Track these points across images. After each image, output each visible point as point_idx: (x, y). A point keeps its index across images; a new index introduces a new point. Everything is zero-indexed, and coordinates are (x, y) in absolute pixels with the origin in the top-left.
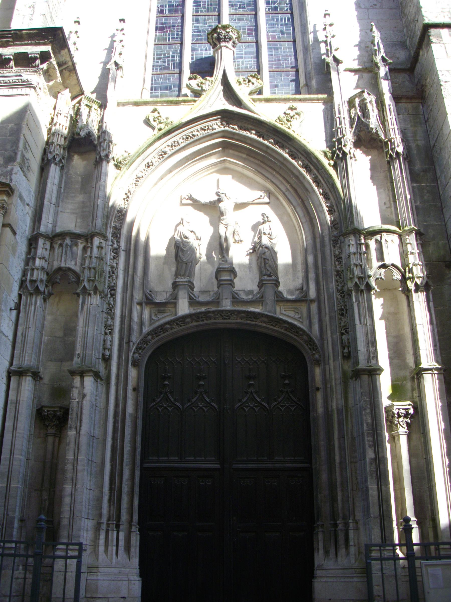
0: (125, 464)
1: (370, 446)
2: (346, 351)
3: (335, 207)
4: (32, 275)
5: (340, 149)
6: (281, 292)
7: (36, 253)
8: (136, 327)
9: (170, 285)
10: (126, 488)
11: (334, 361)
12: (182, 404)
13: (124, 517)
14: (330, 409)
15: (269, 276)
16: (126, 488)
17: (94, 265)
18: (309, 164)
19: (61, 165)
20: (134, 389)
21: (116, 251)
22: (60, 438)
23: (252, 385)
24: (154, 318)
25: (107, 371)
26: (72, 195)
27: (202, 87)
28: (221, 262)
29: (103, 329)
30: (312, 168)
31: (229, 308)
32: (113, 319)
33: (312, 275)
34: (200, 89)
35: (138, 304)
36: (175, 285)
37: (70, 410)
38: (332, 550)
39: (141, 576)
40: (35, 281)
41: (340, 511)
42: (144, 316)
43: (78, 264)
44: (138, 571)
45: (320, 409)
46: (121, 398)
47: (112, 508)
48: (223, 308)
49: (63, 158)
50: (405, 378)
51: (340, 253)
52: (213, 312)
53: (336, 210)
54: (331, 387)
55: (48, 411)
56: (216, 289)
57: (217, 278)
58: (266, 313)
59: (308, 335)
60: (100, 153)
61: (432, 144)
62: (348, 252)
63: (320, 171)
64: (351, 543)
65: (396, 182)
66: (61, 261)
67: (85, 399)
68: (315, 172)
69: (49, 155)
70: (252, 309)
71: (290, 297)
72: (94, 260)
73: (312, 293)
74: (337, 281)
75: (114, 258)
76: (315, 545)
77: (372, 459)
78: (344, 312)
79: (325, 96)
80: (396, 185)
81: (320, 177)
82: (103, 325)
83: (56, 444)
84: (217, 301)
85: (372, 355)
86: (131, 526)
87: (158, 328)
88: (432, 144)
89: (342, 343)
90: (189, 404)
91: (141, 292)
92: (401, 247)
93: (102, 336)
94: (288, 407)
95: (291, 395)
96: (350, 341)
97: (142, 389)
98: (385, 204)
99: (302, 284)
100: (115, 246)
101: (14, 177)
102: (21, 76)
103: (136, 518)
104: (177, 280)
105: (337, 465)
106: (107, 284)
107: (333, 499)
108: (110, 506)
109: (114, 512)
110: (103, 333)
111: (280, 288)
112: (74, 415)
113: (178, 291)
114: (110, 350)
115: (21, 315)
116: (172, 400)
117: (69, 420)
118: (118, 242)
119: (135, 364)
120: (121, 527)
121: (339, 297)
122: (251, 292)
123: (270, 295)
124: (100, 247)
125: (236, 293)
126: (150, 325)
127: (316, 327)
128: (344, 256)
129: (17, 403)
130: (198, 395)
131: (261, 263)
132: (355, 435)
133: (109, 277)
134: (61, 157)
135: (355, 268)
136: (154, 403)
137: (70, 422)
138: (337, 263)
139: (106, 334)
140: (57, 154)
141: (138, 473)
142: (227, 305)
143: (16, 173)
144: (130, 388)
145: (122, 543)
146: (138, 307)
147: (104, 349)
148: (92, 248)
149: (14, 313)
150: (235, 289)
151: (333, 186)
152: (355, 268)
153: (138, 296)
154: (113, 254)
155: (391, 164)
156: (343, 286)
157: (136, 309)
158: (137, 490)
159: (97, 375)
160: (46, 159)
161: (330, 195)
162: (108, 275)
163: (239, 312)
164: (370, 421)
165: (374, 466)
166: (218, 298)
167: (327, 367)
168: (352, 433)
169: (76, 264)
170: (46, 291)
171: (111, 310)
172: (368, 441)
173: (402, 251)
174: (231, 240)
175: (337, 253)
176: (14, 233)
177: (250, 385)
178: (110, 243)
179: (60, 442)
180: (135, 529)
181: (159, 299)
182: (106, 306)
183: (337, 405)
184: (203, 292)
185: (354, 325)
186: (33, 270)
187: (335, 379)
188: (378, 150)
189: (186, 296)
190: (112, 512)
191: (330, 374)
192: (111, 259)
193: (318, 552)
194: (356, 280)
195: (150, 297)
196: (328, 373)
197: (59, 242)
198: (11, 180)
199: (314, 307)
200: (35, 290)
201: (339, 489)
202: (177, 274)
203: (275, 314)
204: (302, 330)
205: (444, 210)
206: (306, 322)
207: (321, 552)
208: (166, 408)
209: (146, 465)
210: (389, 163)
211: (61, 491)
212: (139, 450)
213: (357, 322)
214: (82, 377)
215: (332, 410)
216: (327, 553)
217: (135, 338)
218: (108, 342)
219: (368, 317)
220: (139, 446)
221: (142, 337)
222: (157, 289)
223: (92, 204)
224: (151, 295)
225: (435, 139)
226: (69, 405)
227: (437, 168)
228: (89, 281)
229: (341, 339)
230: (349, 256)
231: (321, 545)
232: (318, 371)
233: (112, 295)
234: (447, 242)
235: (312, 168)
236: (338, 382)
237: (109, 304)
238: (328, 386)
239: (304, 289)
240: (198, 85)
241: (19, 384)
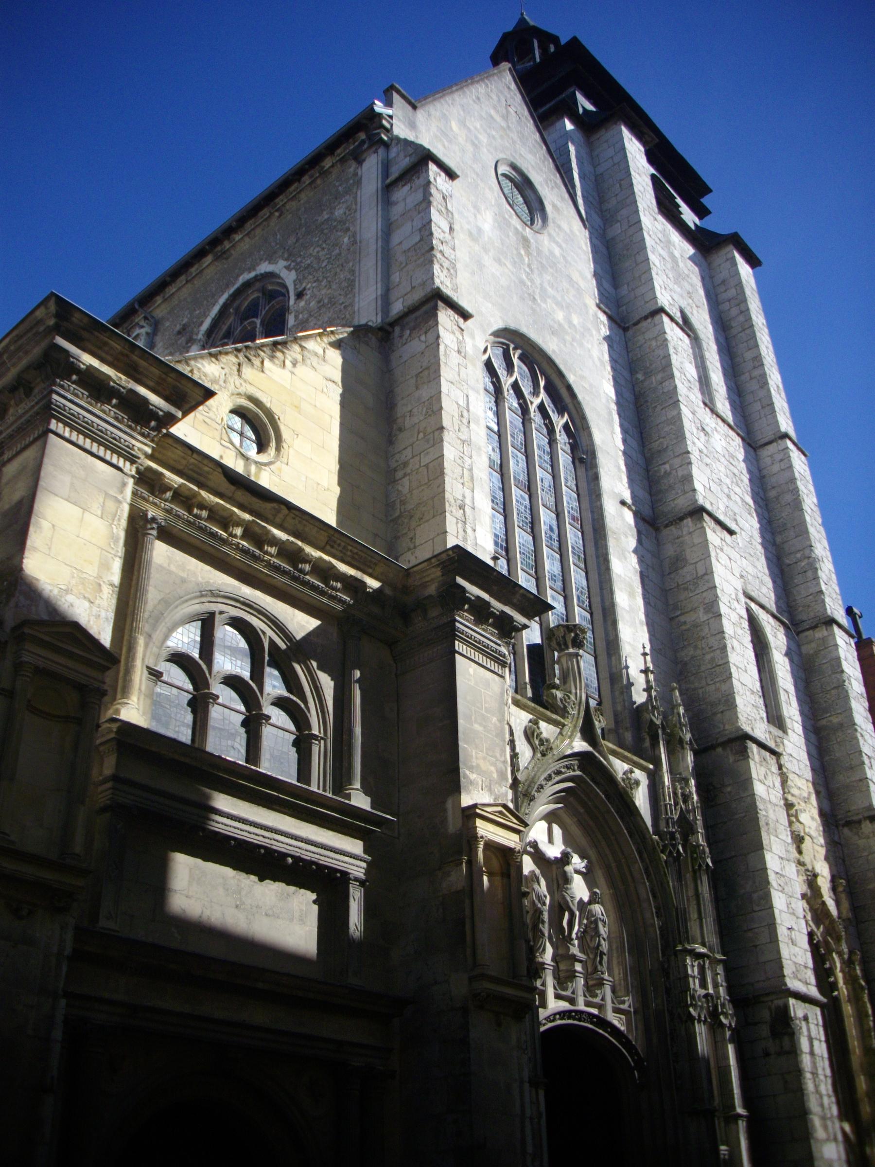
3: (662, 911)
5: (675, 846)
18: (644, 850)
27: (565, 707)
34: (562, 706)
65: (703, 897)
68: (647, 860)
79: (651, 767)
80: (703, 900)
81: (650, 869)
102: (499, 645)
151: (664, 886)
155: (698, 874)
210: (694, 871)
235: (645, 855)
240: (561, 700)
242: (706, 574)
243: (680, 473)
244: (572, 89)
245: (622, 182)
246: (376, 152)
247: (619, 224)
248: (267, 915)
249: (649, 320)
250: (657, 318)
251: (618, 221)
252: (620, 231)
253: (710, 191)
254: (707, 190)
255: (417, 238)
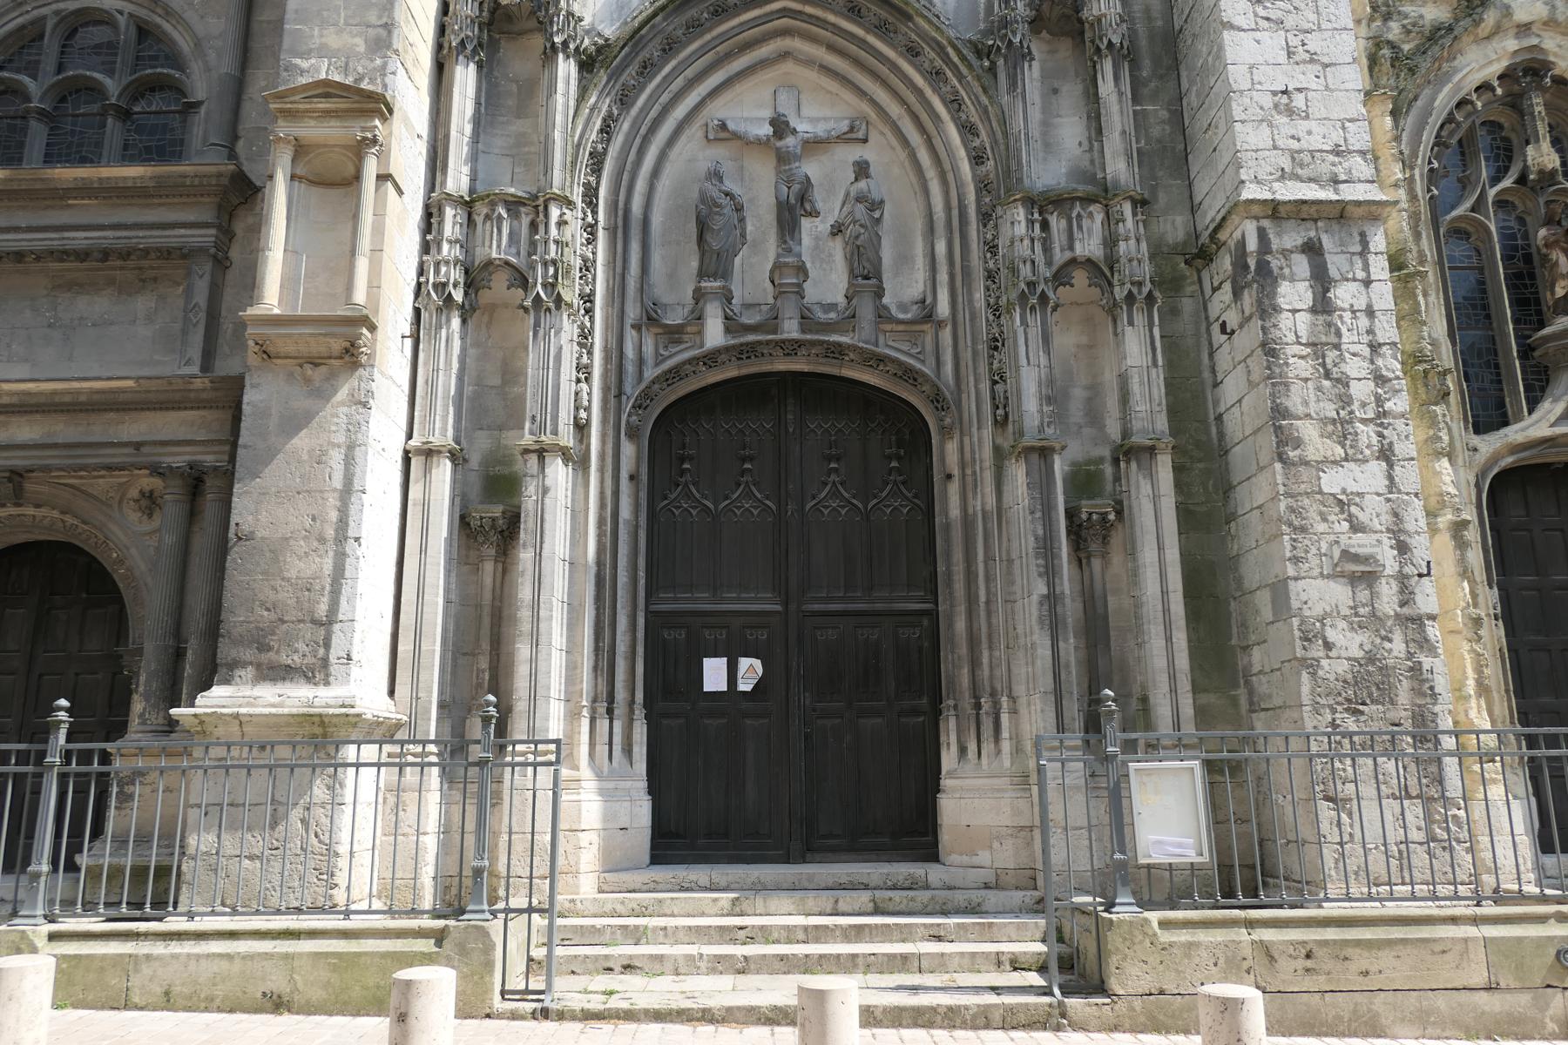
0: (619, 606)
1: (1040, 575)
2: (1000, 412)
4: (437, 272)
6: (886, 308)
7: (440, 232)
8: (630, 368)
9: (690, 293)
10: (622, 647)
11: (979, 428)
12: (716, 504)
13: (621, 694)
14: (970, 511)
15: (866, 278)
16: (622, 647)
17: (553, 254)
18: (944, 66)
19: (477, 58)
20: (632, 478)
21: (591, 229)
22: (504, 563)
23: (836, 470)
24: (662, 352)
25: (584, 447)
26: (501, 119)
28: (780, 250)
29: (574, 373)
30: (949, 74)
31: (795, 335)
32: (590, 353)
33: (943, 277)
35: (633, 326)
36: (699, 295)
37: (523, 515)
38: (972, 747)
39: (649, 793)
40: (444, 285)
41: (986, 682)
42: (644, 348)
43: (523, 253)
44: (643, 784)
45: (955, 512)
46: (609, 493)
47: (600, 680)
48: (785, 336)
49: (480, 45)
50: (1101, 460)
51: (995, 237)
52: (768, 342)
53: (990, 156)
54: (974, 473)
55: (481, 518)
56: (771, 301)
57: (773, 282)
58: (861, 345)
59: (935, 385)
60: (552, 36)
61: (1177, 27)
62: (1009, 234)
63: (964, 82)
64: (1005, 734)
66: (491, 247)
67: (549, 495)
69: (452, 37)
70: (835, 338)
71: (901, 316)
72: (553, 247)
73: (943, 308)
74: (987, 289)
75: (589, 242)
76: (943, 738)
77: (1043, 596)
78: (999, 344)
81: (963, 93)
82: (574, 365)
83: (499, 575)
84: (772, 323)
85: (1046, 420)
86: (632, 711)
87: (670, 371)
88: (1177, 27)
89: (994, 398)
90: (727, 502)
91: (639, 305)
92: (1106, 227)
93: (574, 384)
94: (895, 508)
95: (902, 487)
96: (1009, 395)
97: (644, 477)
98: (1080, 144)
99: (924, 292)
100: (590, 219)
101: (389, 79)
103: (639, 696)
104: (703, 284)
105: (982, 606)
106: (577, 292)
107: (975, 664)
108: (596, 678)
109: (603, 688)
110: (574, 379)
111: (885, 300)
112: (531, 524)
113: (705, 303)
114: (588, 409)
115: (421, 346)
116: (697, 495)
117: (522, 532)
118: (595, 213)
119: (633, 434)
120: (616, 712)
121: (991, 318)
122: (832, 307)
123: (866, 311)
124: (562, 223)
125: (808, 310)
126: (657, 365)
127: (948, 368)
128: (1002, 243)
129: (425, 506)
130: (742, 487)
131: (852, 254)
132: (1014, 555)
133: (581, 278)
134: (475, 42)
135: (1021, 266)
136: (666, 502)
137: (522, 535)
138: (989, 255)
139: (578, 381)
140: (467, 37)
141: (641, 621)
142: (791, 329)
143: (394, 73)
144: (624, 475)
145: (617, 739)
146: (634, 333)
147: (577, 409)
148: (547, 225)
149: (409, 343)
150: (805, 300)
152: (1021, 266)
153: (633, 312)
154: (585, 234)
156: (998, 297)
157: (630, 336)
158: (640, 650)
159: (565, 454)
160: (446, 45)
161: (980, 126)
162: (578, 275)
163: (813, 343)
164: (1040, 532)
165: (1046, 607)
166: (776, 318)
167: (967, 440)
168: (1008, 552)
169: (518, 253)
170: (466, 303)
171: (586, 338)
172: (1037, 565)
173: (1107, 233)
174: (799, 211)
175: (989, 236)
176: (400, 192)
177: (831, 471)
178: (580, 215)
179: (505, 571)
180: (639, 713)
181: (673, 319)
182: (577, 331)
183: (983, 504)
184: (747, 306)
185: (1018, 368)
186: (437, 265)
187: (981, 461)
188: (1073, 38)
189: (720, 313)
190: (600, 687)
191: (973, 452)
192: (582, 245)
193: (949, 748)
194: (1023, 286)
195: (655, 315)
196: (967, 449)
197: (485, 211)
198: (385, 86)
199: (946, 335)
200: (444, 301)
201: (985, 645)
202: (702, 274)
203: (877, 346)
204: (924, 375)
205: (1190, 157)
206: (931, 361)
207: (954, 748)
208: (686, 509)
209: (653, 608)
211: (511, 655)
212: (642, 582)
213: (1023, 361)
214: (541, 459)
215: (975, 514)
216: (963, 750)
217: (632, 390)
218: (585, 396)
219: (1041, 353)
220: (642, 574)
221: (643, 386)
222: (666, 299)
223: (542, 139)
224: (656, 312)
225: (1184, 17)
226: (520, 507)
227: (1184, 74)
228: (544, 285)
229: (993, 391)
230: (1012, 243)
231: (953, 738)
232: (952, 447)
233: (587, 311)
234: (1191, 217)
235: (949, 74)
236: (987, 464)
237: (582, 327)
238: (969, 471)
239: (928, 302)
241: (427, 471)
248: (93, 325)
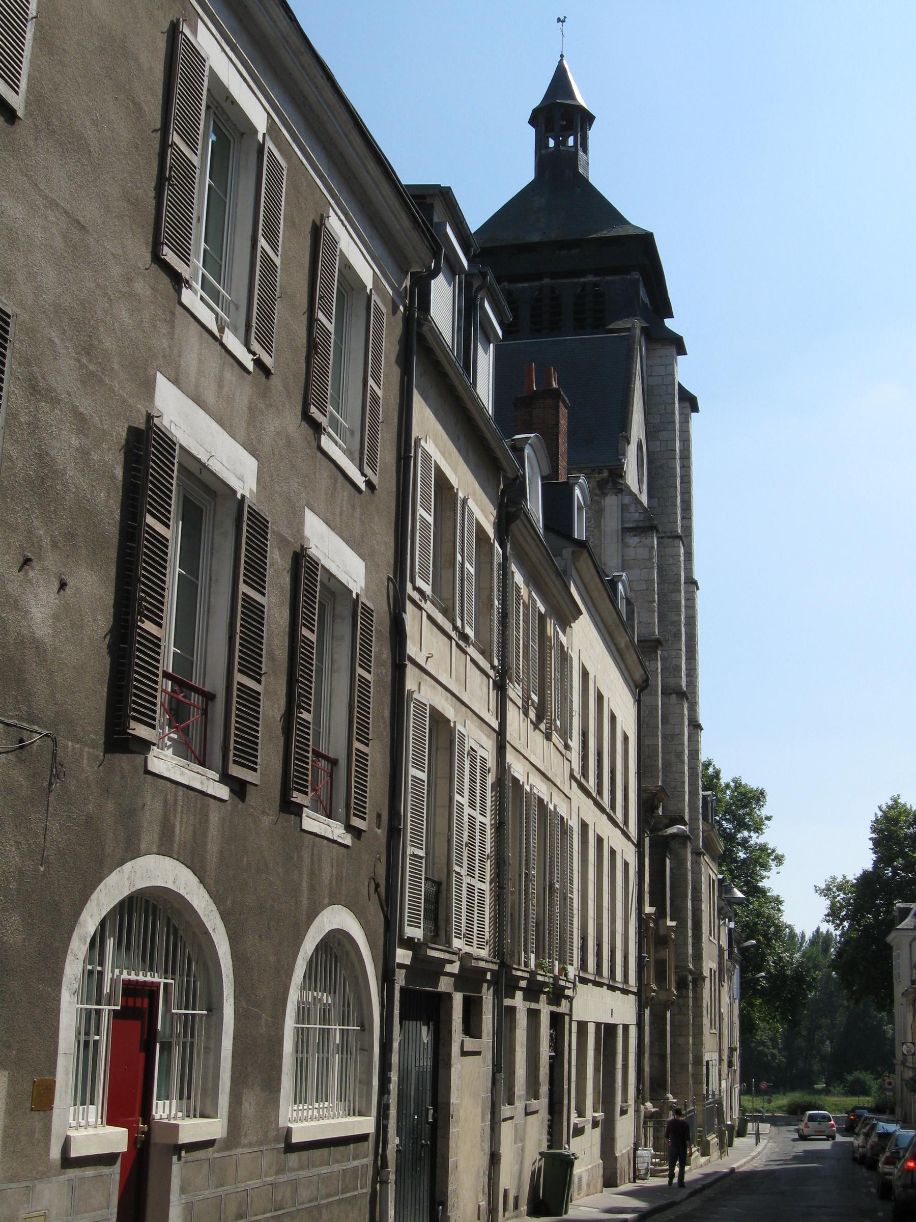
242: (679, 734)
243: (674, 663)
244: (636, 275)
245: (667, 406)
246: (616, 494)
247: (658, 442)
249: (671, 540)
250: (677, 541)
251: (658, 439)
252: (659, 450)
253: (672, 317)
254: (671, 316)
255: (644, 587)
